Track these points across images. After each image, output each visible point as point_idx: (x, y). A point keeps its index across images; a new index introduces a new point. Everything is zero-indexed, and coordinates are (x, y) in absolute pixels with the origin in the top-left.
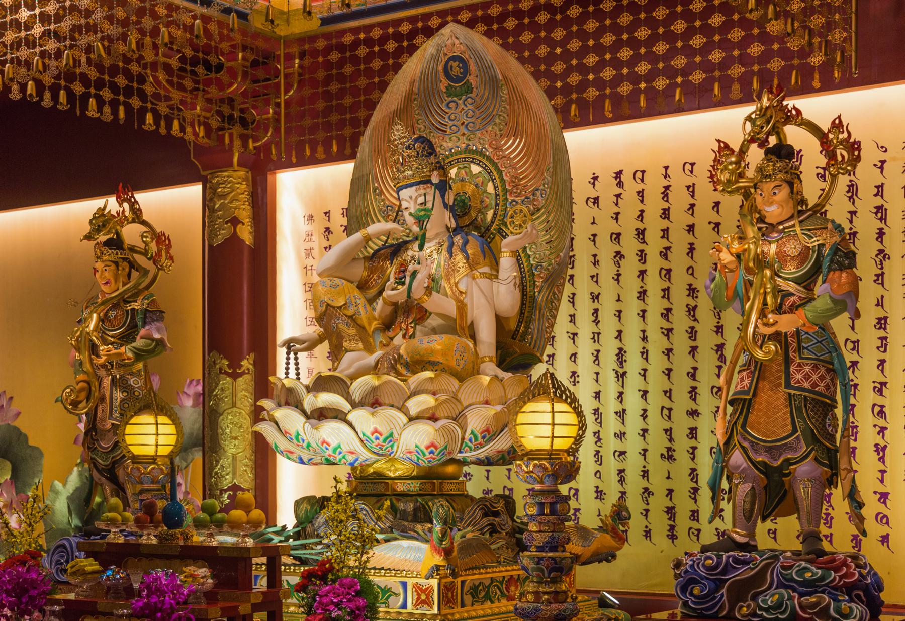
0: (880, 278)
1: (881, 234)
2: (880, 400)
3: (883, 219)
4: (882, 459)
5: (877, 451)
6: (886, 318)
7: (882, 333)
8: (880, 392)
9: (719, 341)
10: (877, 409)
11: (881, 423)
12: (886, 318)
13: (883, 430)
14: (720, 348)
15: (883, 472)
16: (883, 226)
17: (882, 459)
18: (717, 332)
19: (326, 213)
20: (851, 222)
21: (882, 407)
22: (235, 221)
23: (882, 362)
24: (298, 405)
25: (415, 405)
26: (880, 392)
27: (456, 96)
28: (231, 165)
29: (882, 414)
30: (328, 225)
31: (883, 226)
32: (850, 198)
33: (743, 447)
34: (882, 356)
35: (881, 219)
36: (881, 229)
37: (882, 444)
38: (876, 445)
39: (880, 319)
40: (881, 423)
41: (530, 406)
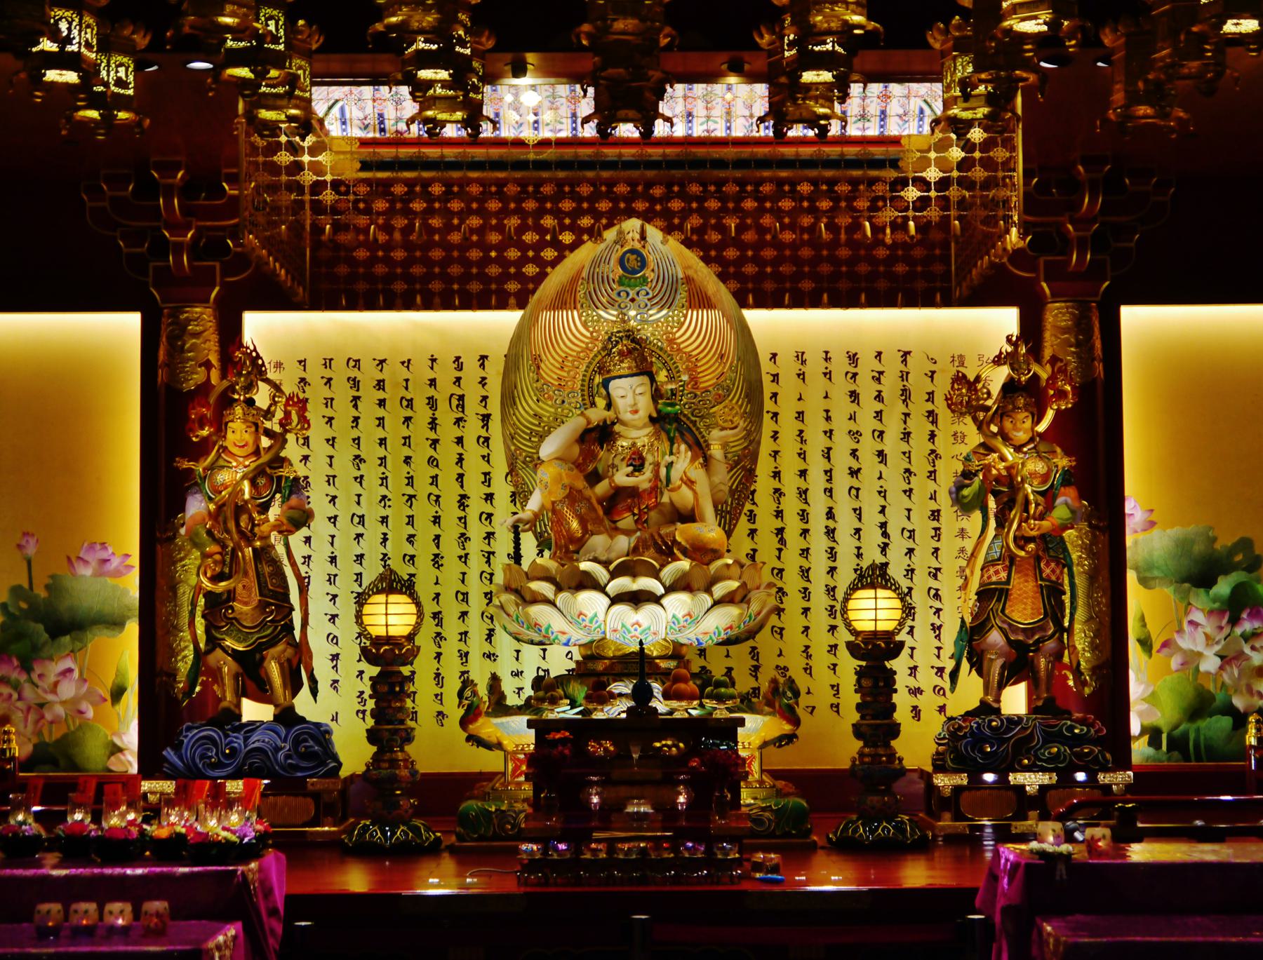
0: (932, 474)
1: (932, 436)
2: (935, 584)
3: (934, 422)
4: (938, 637)
5: (934, 629)
6: (938, 511)
7: (935, 524)
8: (935, 577)
9: (779, 524)
10: (933, 592)
11: (937, 604)
12: (938, 511)
13: (938, 611)
14: (780, 531)
15: (939, 648)
16: (934, 428)
17: (938, 637)
18: (777, 517)
19: (300, 362)
20: (905, 422)
21: (937, 590)
22: (208, 365)
23: (937, 550)
24: (602, 589)
25: (720, 590)
26: (935, 577)
27: (629, 286)
28: (208, 301)
29: (937, 596)
30: (303, 375)
31: (934, 428)
32: (904, 401)
33: (1000, 628)
34: (937, 545)
35: (932, 423)
36: (932, 432)
37: (938, 623)
38: (933, 625)
39: (933, 512)
40: (937, 604)
41: (860, 594)
